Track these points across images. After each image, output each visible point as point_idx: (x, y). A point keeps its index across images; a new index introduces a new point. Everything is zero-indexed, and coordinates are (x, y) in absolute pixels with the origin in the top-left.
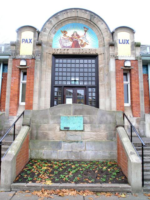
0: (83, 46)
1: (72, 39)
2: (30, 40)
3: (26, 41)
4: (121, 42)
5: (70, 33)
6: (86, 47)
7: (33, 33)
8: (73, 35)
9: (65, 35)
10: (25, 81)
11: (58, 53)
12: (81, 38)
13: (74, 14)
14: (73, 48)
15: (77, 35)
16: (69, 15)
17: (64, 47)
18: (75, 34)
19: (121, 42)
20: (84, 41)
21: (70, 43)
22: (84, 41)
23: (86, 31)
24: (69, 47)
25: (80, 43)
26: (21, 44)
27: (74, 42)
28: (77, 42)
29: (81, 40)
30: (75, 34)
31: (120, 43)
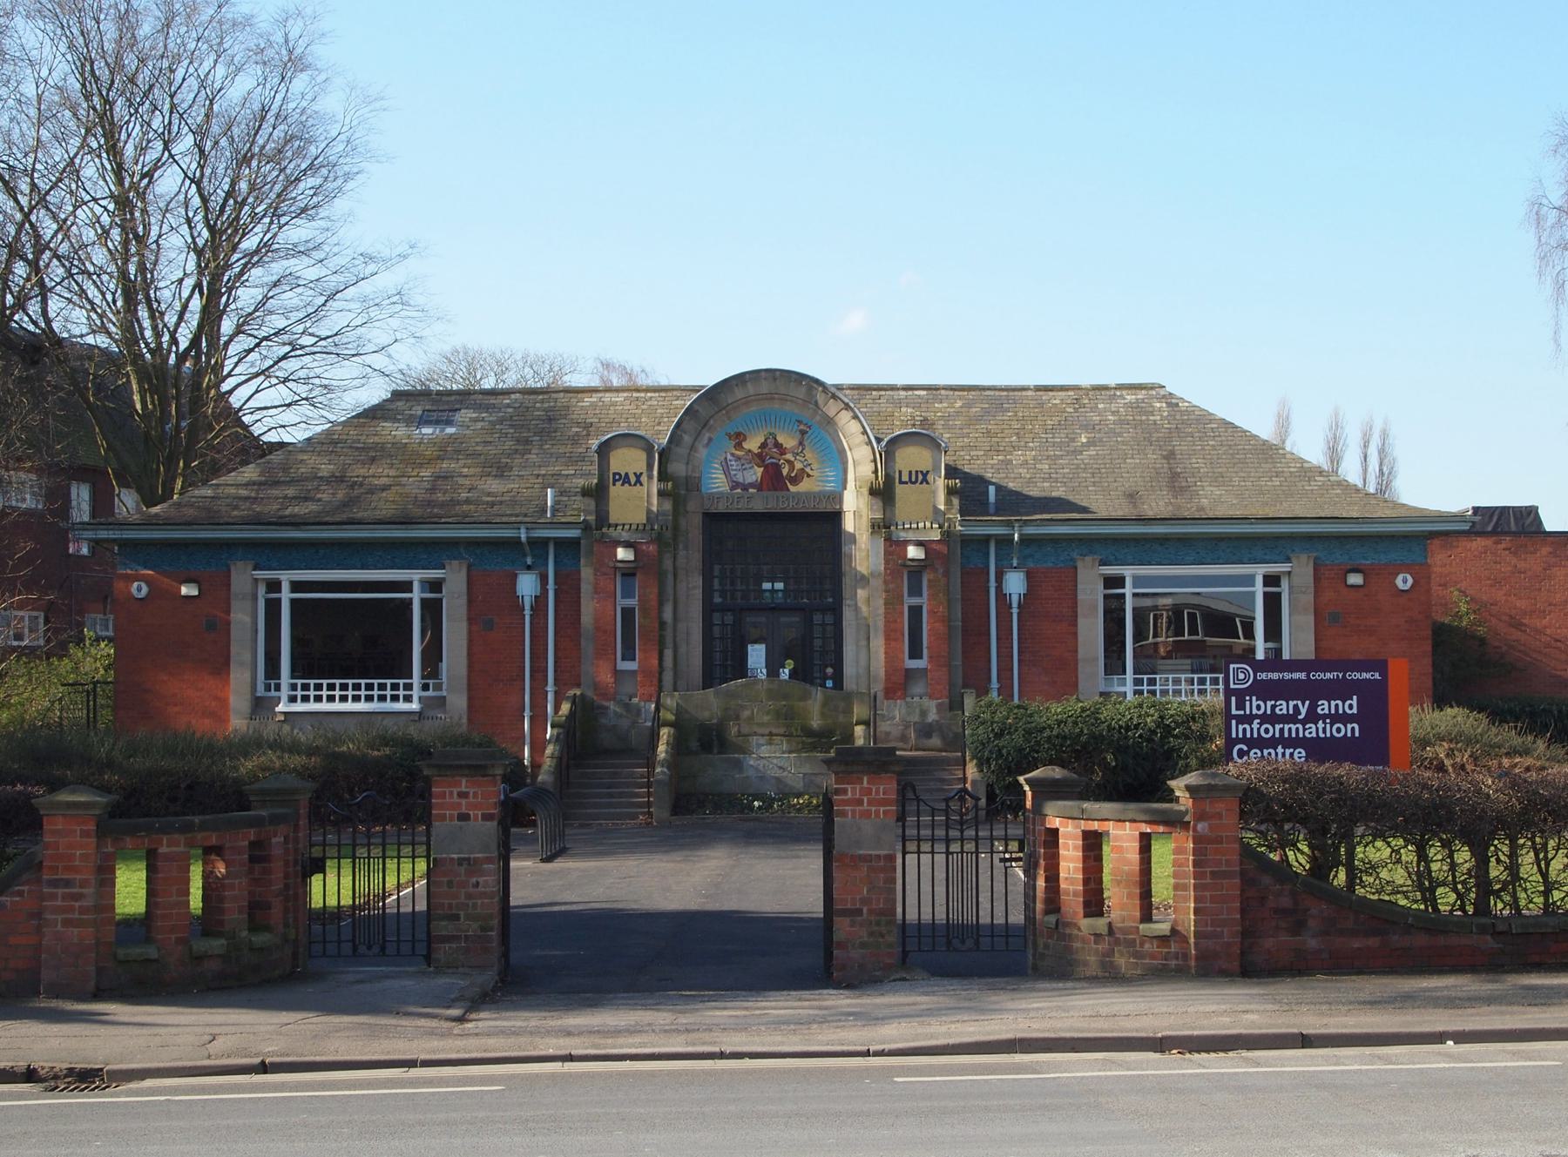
0: (795, 480)
1: (760, 458)
2: (638, 476)
3: (626, 480)
4: (905, 478)
5: (753, 444)
6: (804, 486)
7: (643, 456)
8: (763, 446)
9: (739, 446)
10: (632, 602)
11: (721, 508)
12: (789, 456)
13: (765, 387)
14: (765, 493)
15: (778, 445)
16: (751, 389)
17: (736, 485)
18: (770, 442)
19: (905, 478)
20: (798, 466)
21: (756, 474)
22: (798, 466)
23: (803, 433)
24: (752, 485)
25: (785, 471)
26: (612, 488)
27: (766, 467)
28: (777, 467)
29: (788, 461)
30: (770, 442)
31: (901, 482)
